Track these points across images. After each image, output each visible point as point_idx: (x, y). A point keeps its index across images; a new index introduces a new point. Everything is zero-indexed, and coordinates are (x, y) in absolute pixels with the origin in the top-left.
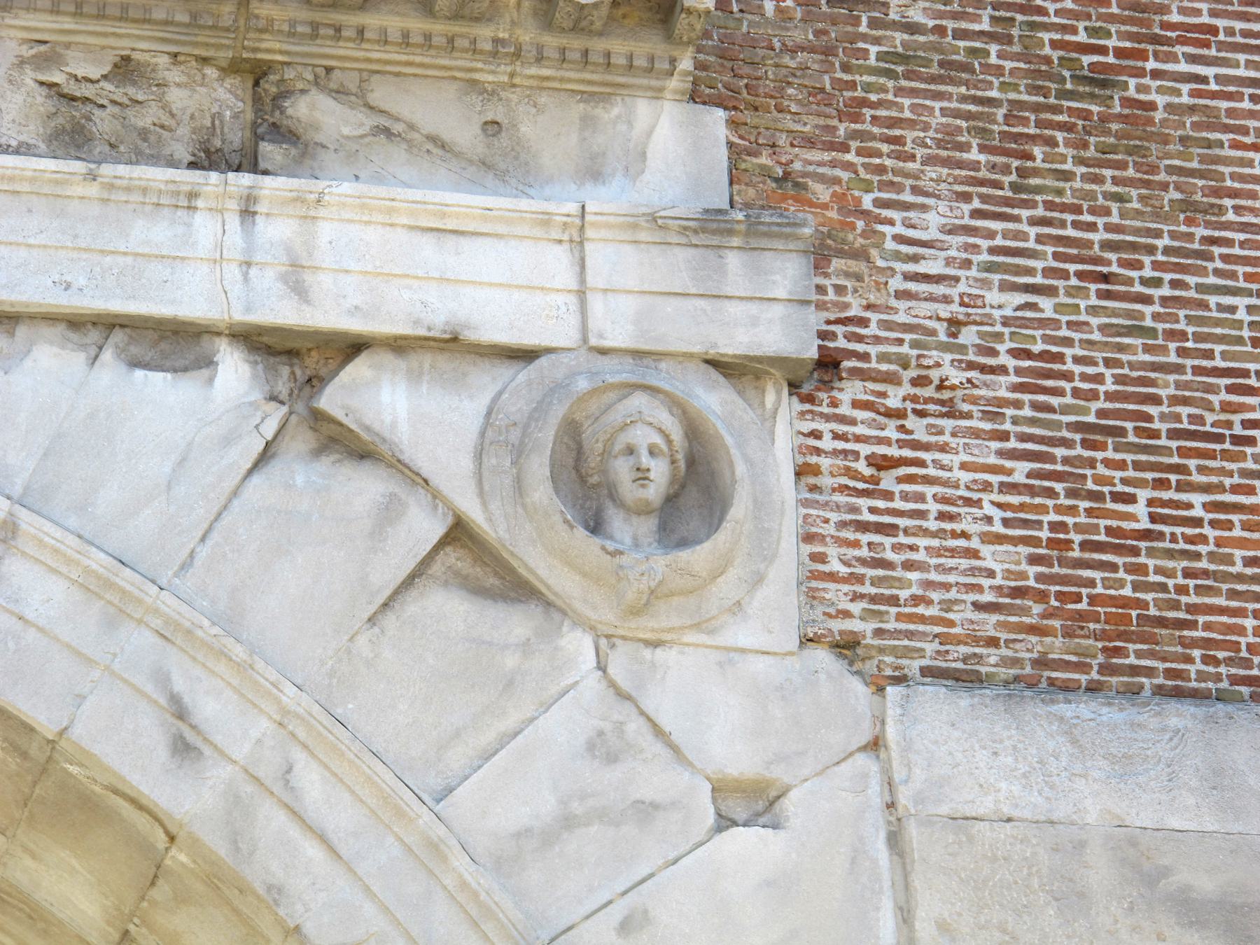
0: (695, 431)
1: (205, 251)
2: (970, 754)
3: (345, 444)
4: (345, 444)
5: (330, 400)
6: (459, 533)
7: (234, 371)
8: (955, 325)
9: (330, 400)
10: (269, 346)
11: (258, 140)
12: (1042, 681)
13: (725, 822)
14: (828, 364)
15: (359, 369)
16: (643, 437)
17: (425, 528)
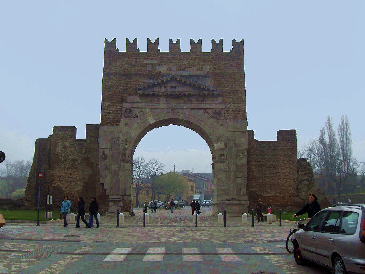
0: (220, 111)
1: (202, 106)
2: (230, 124)
3: (207, 112)
4: (207, 112)
5: (207, 111)
6: (211, 116)
7: (203, 110)
8: (231, 105)
9: (207, 111)
10: (204, 109)
11: (203, 101)
12: (233, 120)
13: (221, 126)
14: (225, 108)
15: (207, 110)
16: (218, 112)
17: (210, 116)
